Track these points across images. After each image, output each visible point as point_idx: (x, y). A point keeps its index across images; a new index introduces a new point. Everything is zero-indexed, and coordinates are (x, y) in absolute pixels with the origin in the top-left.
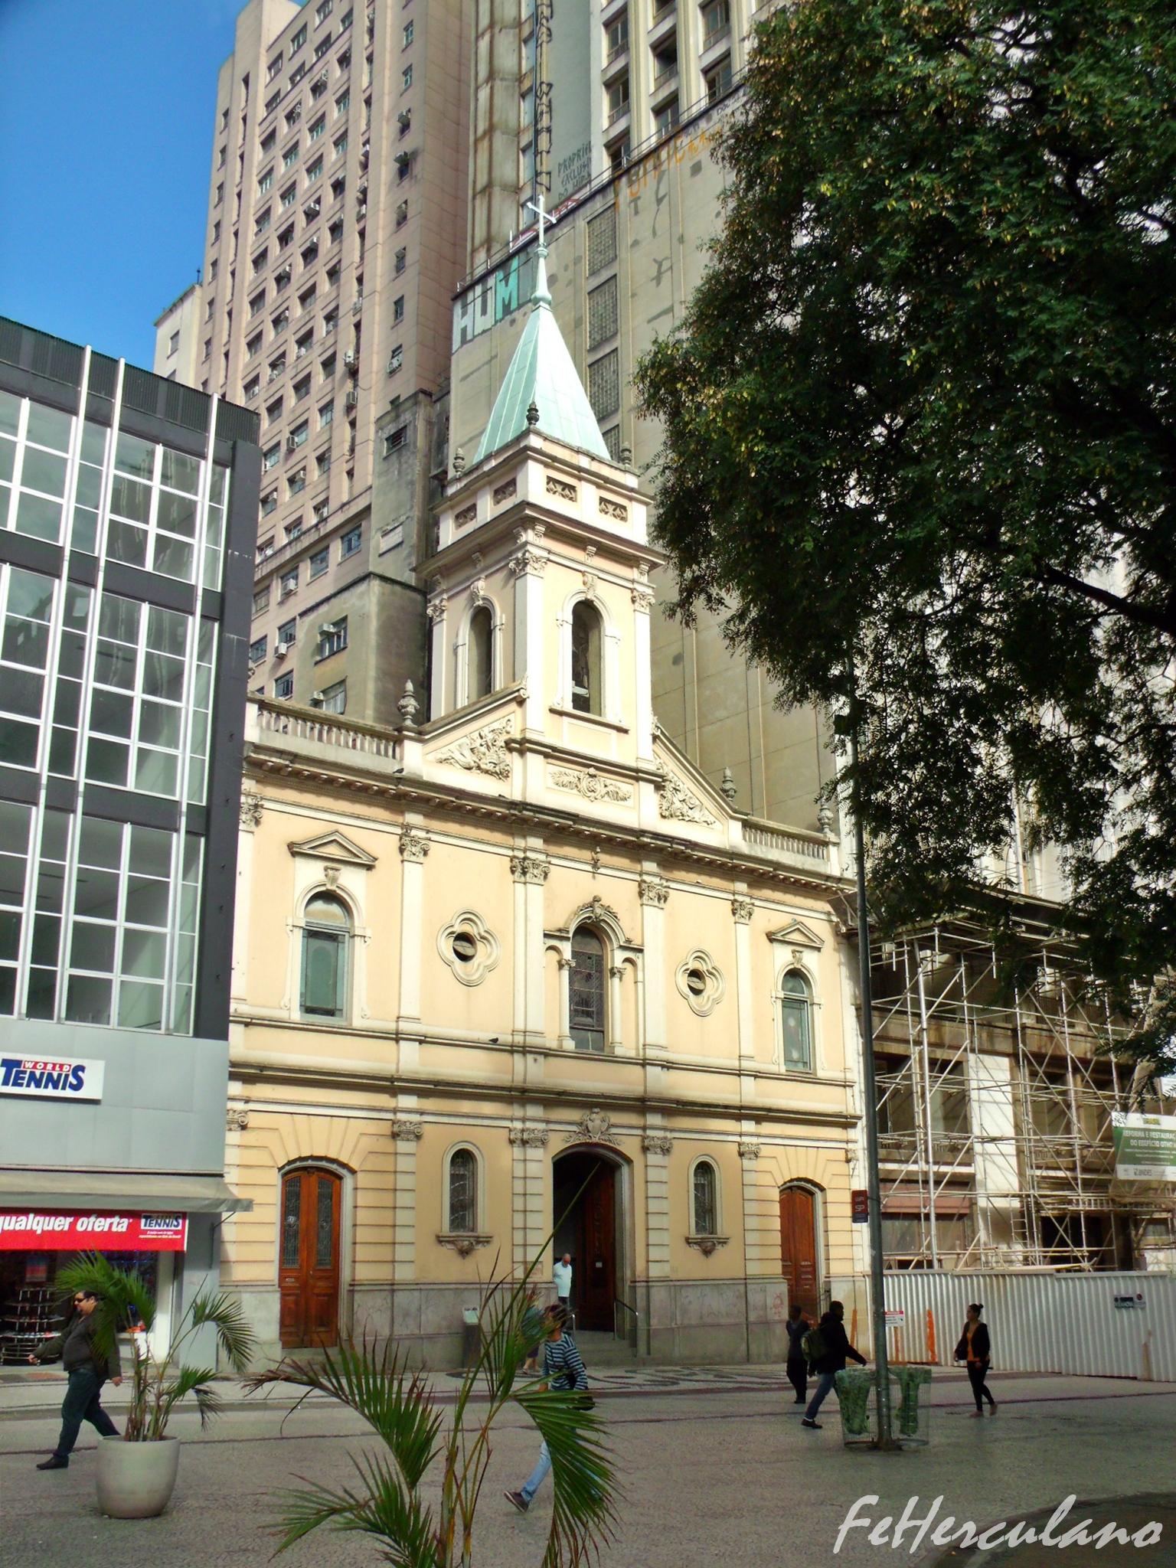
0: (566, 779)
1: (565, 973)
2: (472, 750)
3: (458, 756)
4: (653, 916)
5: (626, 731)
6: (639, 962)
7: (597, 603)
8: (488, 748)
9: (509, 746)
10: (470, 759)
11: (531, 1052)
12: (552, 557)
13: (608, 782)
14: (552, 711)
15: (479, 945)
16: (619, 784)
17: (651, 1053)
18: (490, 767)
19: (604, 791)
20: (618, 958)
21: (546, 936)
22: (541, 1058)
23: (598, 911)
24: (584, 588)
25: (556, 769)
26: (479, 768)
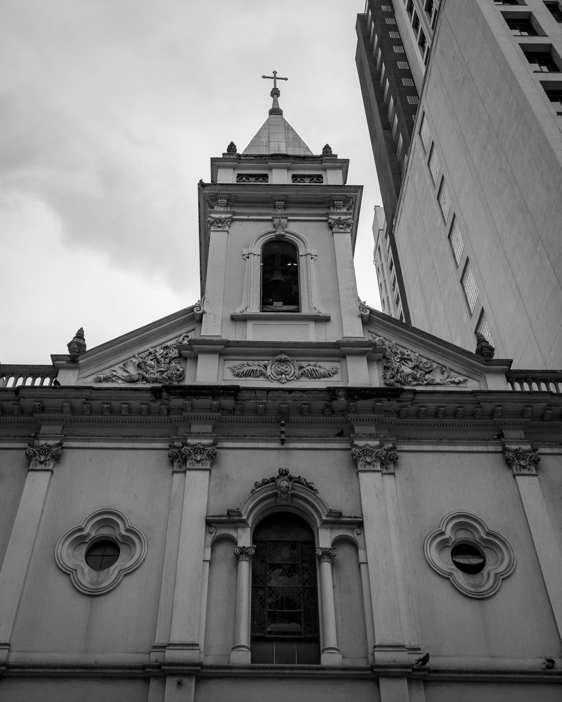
0: (246, 369)
1: (245, 567)
2: (139, 366)
3: (121, 373)
4: (370, 481)
5: (326, 320)
6: (359, 539)
7: (289, 236)
8: (158, 362)
9: (181, 357)
10: (133, 371)
11: (173, 674)
12: (235, 217)
13: (304, 364)
14: (234, 319)
15: (123, 550)
16: (319, 364)
17: (382, 657)
18: (157, 375)
19: (298, 373)
20: (325, 539)
21: (210, 523)
22: (191, 684)
23: (284, 483)
24: (272, 229)
25: (237, 363)
26: (144, 378)
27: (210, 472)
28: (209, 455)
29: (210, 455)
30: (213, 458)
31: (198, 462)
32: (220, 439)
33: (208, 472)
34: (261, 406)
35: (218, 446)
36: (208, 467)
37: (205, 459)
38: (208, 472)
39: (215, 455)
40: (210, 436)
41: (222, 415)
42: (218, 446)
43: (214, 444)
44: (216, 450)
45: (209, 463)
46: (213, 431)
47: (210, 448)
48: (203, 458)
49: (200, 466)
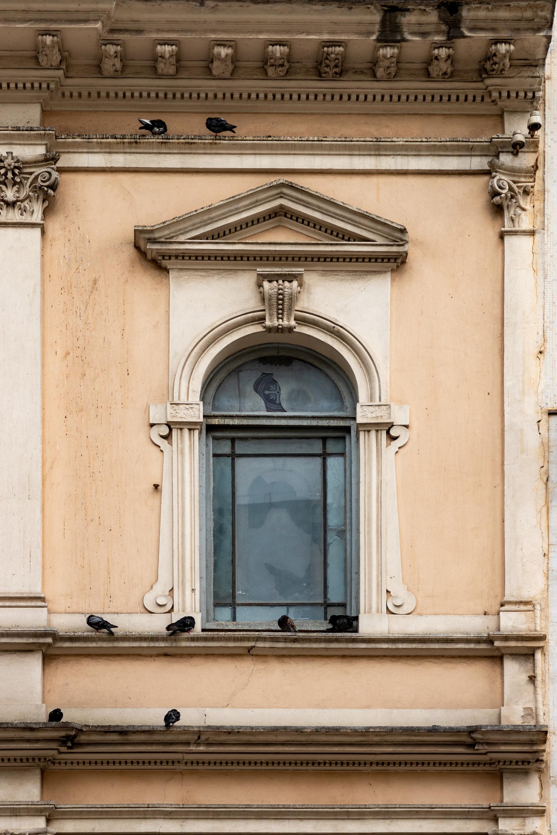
27: (43, 233)
28: (35, 189)
29: (41, 188)
30: (48, 195)
31: (11, 205)
32: (65, 145)
33: (37, 232)
34: (168, 48)
35: (60, 164)
36: (37, 217)
37: (28, 197)
38: (37, 232)
39: (54, 187)
40: (42, 137)
41: (67, 77)
42: (60, 164)
43: (50, 159)
44: (55, 174)
45: (38, 208)
46: (43, 122)
47: (37, 171)
48: (22, 196)
49: (14, 216)
